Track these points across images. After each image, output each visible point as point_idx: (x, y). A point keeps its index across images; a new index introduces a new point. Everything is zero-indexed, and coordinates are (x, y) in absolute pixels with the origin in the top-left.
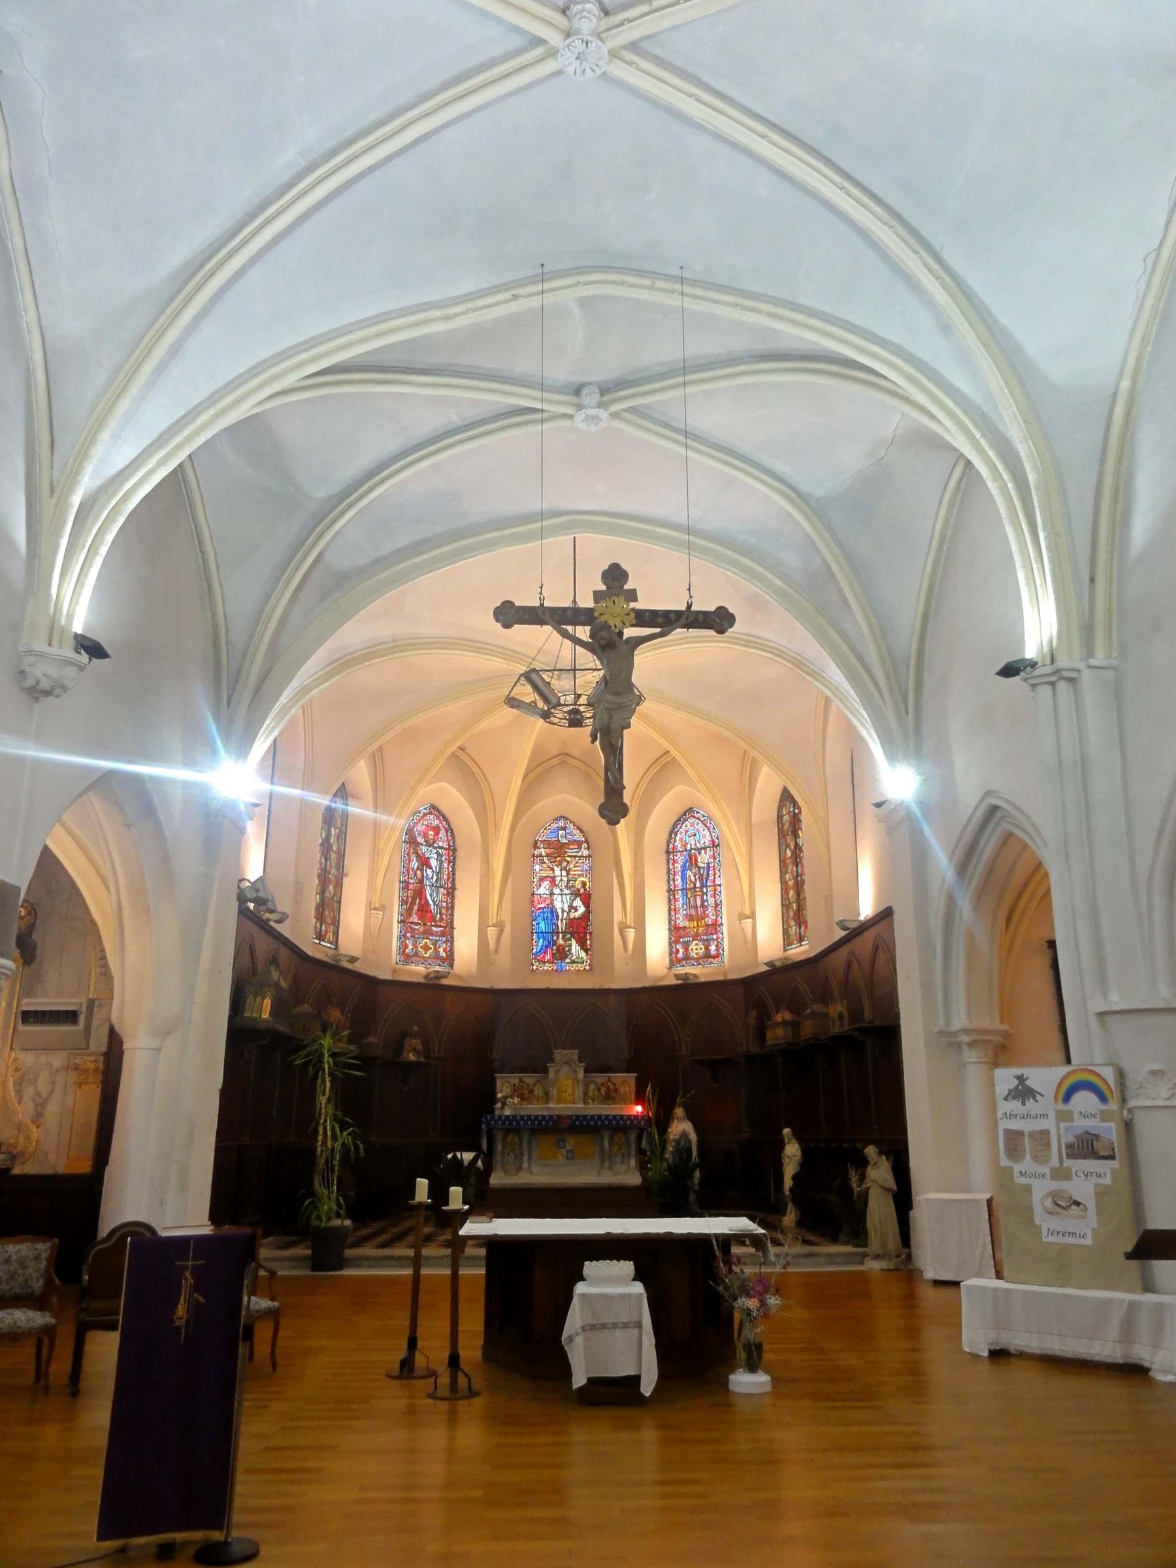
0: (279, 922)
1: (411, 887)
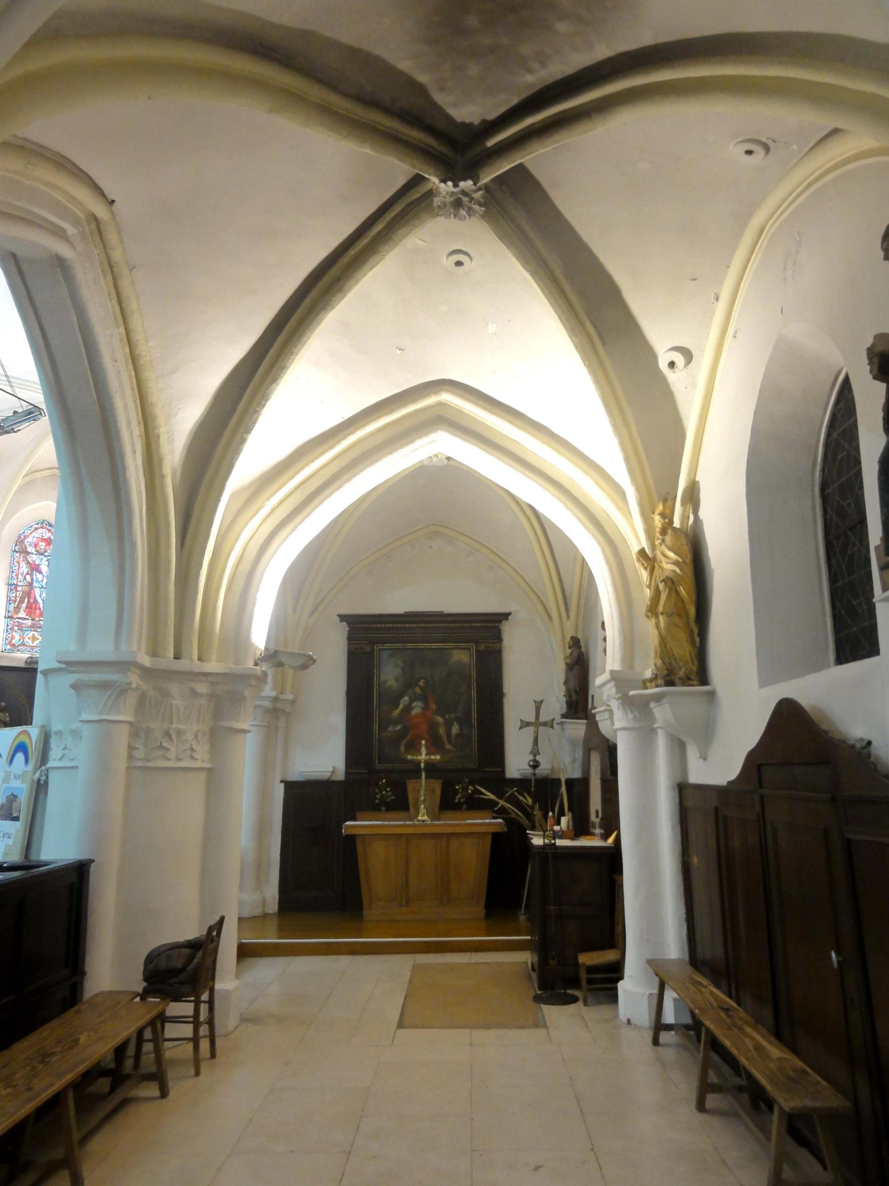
1: (19, 588)
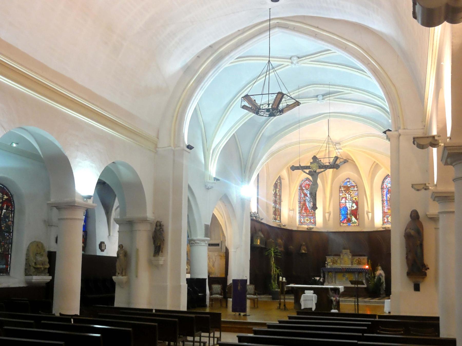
0: (262, 220)
